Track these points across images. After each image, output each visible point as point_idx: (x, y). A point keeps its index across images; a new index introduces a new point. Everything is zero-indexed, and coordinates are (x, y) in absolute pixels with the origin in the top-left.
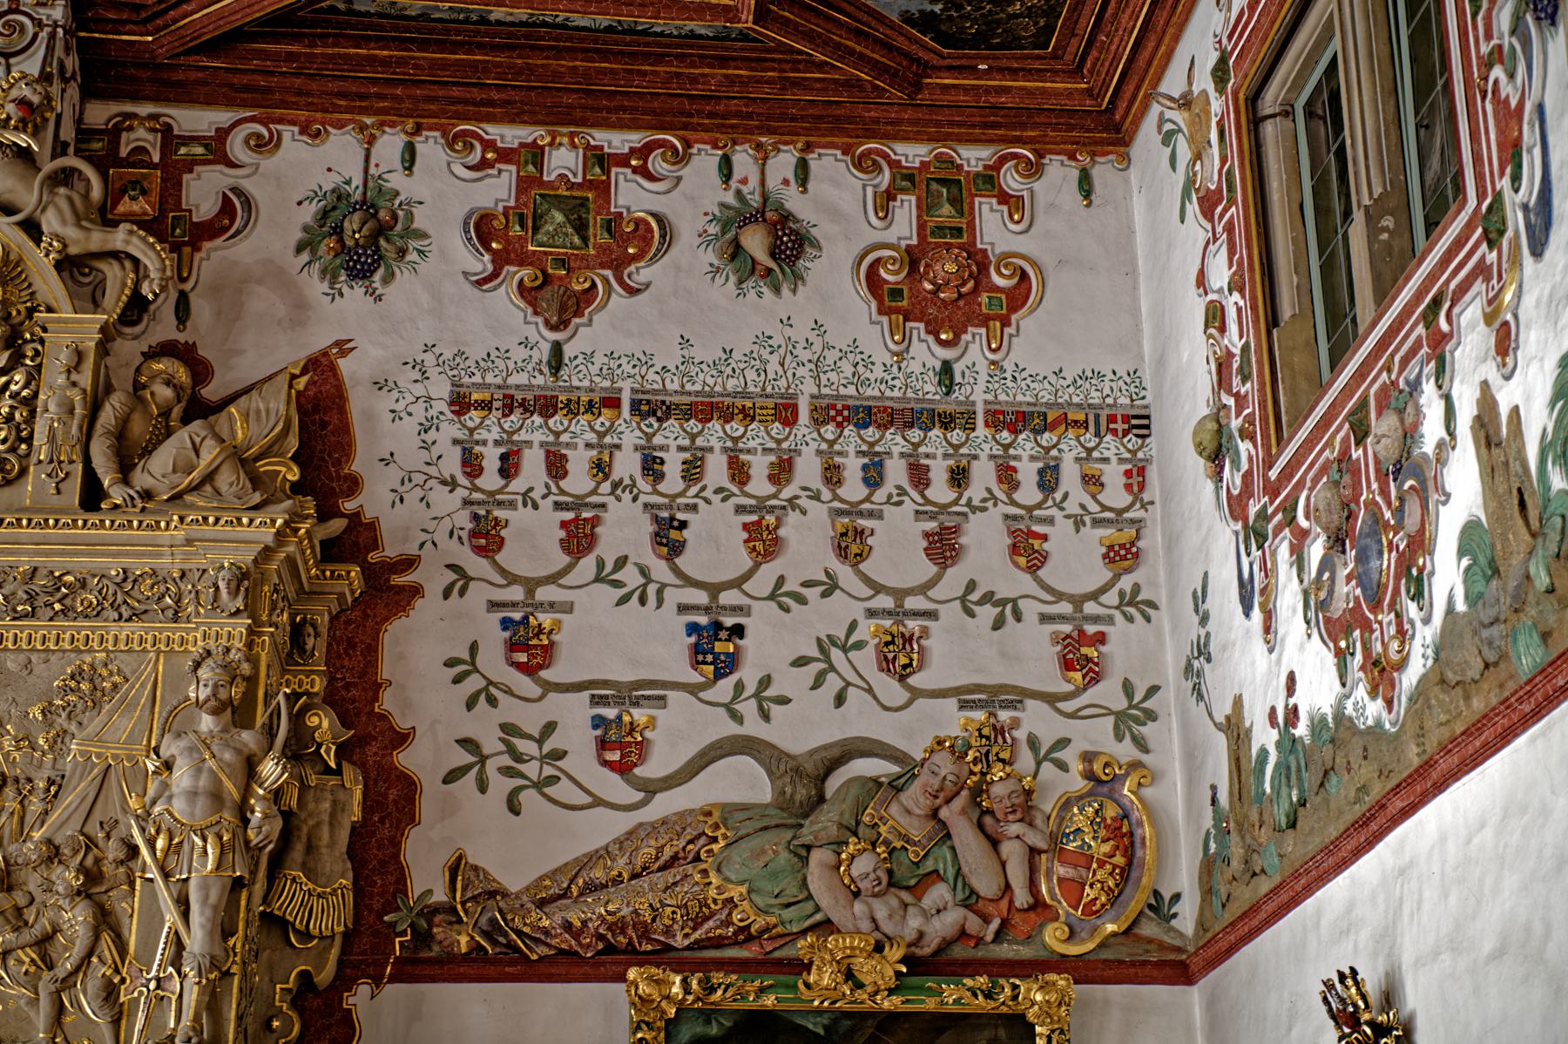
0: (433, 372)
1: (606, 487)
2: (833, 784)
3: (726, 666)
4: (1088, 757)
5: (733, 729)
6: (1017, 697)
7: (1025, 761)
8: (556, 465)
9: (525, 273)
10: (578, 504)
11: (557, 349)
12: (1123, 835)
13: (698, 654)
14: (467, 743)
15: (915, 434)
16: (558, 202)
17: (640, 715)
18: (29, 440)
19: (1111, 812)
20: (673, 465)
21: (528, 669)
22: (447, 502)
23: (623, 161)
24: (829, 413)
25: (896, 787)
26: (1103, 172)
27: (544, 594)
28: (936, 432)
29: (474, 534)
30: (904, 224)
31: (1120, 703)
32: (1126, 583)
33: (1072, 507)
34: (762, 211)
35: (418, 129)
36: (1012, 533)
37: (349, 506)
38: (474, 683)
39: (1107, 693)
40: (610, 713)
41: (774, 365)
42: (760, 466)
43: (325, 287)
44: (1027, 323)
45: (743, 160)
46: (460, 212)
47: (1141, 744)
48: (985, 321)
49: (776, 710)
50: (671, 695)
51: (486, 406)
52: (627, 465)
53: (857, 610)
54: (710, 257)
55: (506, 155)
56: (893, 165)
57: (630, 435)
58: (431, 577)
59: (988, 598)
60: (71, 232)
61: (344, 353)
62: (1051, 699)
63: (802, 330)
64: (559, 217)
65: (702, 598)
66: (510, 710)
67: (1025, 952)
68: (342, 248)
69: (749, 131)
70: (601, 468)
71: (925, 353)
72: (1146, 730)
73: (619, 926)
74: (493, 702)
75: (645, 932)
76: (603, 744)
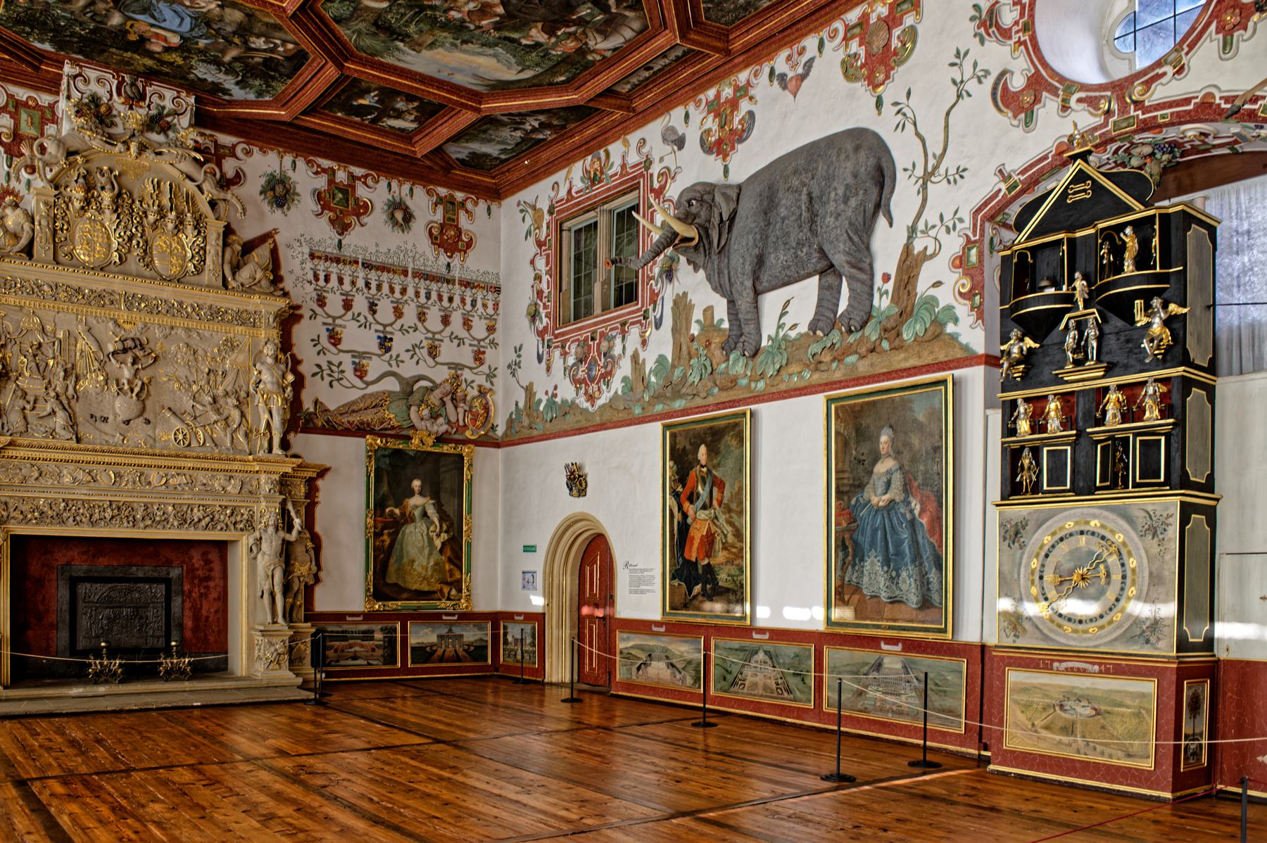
0: (304, 244)
1: (354, 290)
2: (415, 387)
3: (388, 350)
4: (480, 386)
5: (390, 369)
6: (462, 367)
7: (464, 386)
8: (341, 281)
9: (331, 214)
10: (346, 294)
11: (340, 241)
12: (486, 408)
13: (381, 345)
14: (318, 366)
15: (440, 284)
16: (341, 190)
17: (364, 362)
18: (204, 261)
19: (484, 402)
20: (373, 286)
21: (335, 345)
22: (310, 288)
23: (359, 179)
24: (419, 275)
25: (432, 390)
26: (494, 207)
27: (338, 322)
28: (445, 285)
29: (318, 300)
30: (439, 216)
31: (487, 372)
32: (491, 337)
33: (479, 313)
34: (400, 204)
35: (297, 157)
36: (464, 319)
37: (281, 286)
38: (319, 347)
39: (484, 368)
40: (357, 360)
41: (402, 257)
42: (398, 289)
43: (269, 208)
44: (471, 253)
45: (394, 184)
46: (310, 189)
47: (492, 383)
48: (460, 251)
49: (401, 364)
50: (374, 357)
51: (320, 258)
52: (361, 283)
53: (422, 337)
54: (384, 217)
55: (324, 171)
56: (437, 194)
57: (361, 273)
58: (305, 312)
59: (456, 337)
60: (214, 192)
61: (276, 233)
62: (471, 368)
63: (409, 247)
64: (340, 195)
65: (381, 328)
66: (329, 357)
67: (460, 437)
68: (275, 196)
69: (397, 175)
70: (353, 283)
71: (443, 259)
72: (494, 380)
73: (363, 423)
74: (324, 354)
75: (369, 425)
76: (356, 370)
